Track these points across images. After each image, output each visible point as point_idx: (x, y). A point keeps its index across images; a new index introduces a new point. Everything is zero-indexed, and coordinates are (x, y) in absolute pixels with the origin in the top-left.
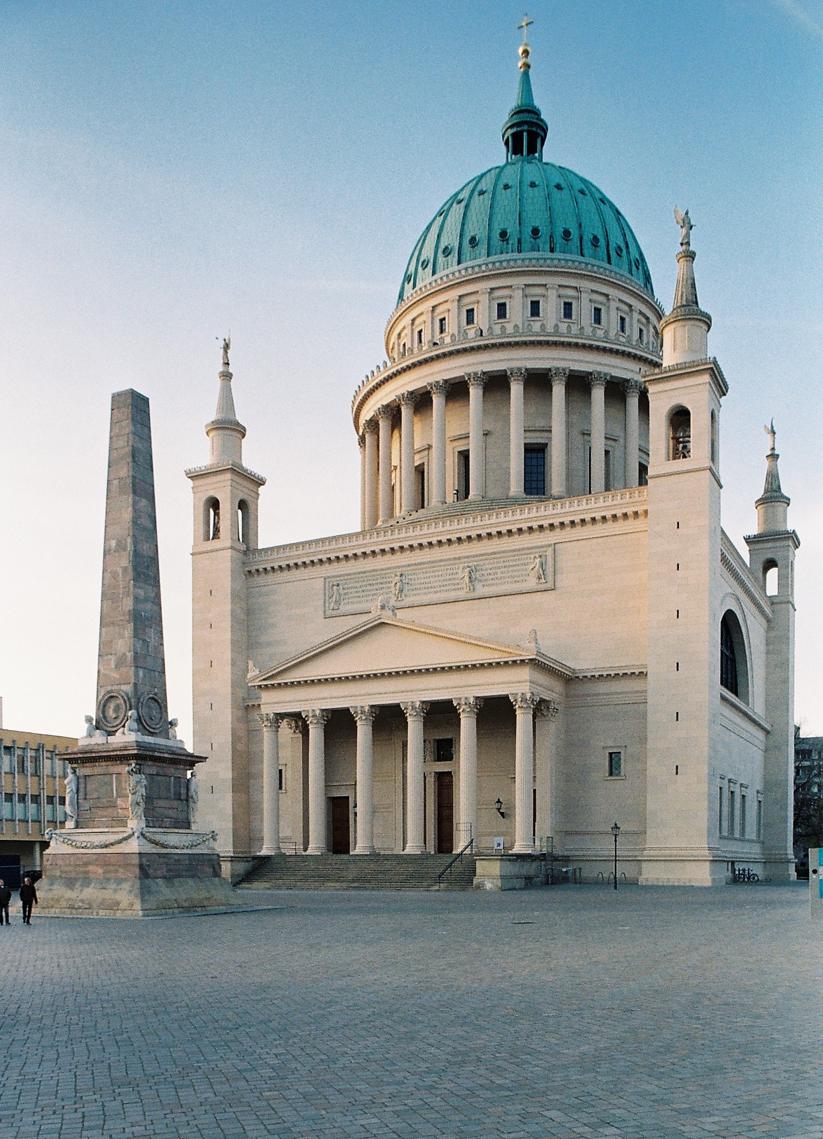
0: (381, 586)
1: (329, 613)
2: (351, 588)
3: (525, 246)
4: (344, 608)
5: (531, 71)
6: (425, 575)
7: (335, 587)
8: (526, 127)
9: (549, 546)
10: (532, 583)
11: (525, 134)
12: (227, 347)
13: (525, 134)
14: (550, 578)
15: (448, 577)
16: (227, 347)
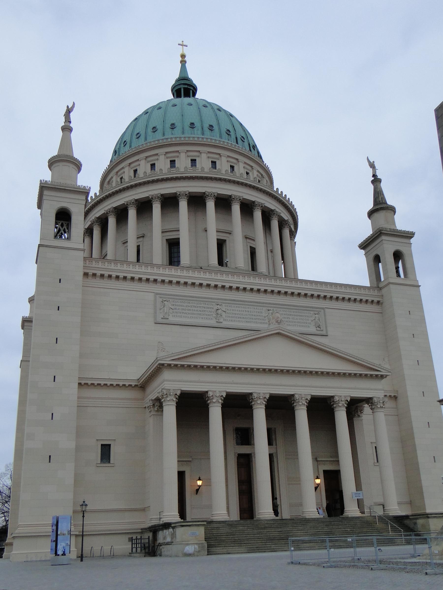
0: (203, 309)
1: (159, 320)
2: (177, 305)
3: (239, 141)
4: (172, 319)
5: (186, 65)
6: (238, 309)
7: (165, 302)
8: (192, 88)
9: (323, 309)
10: (313, 329)
11: (191, 91)
12: (69, 111)
13: (191, 91)
14: (323, 327)
15: (255, 314)
16: (69, 111)
